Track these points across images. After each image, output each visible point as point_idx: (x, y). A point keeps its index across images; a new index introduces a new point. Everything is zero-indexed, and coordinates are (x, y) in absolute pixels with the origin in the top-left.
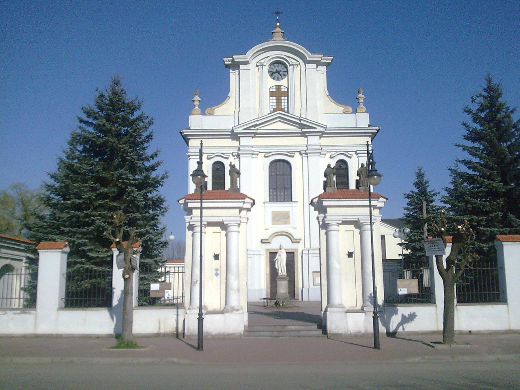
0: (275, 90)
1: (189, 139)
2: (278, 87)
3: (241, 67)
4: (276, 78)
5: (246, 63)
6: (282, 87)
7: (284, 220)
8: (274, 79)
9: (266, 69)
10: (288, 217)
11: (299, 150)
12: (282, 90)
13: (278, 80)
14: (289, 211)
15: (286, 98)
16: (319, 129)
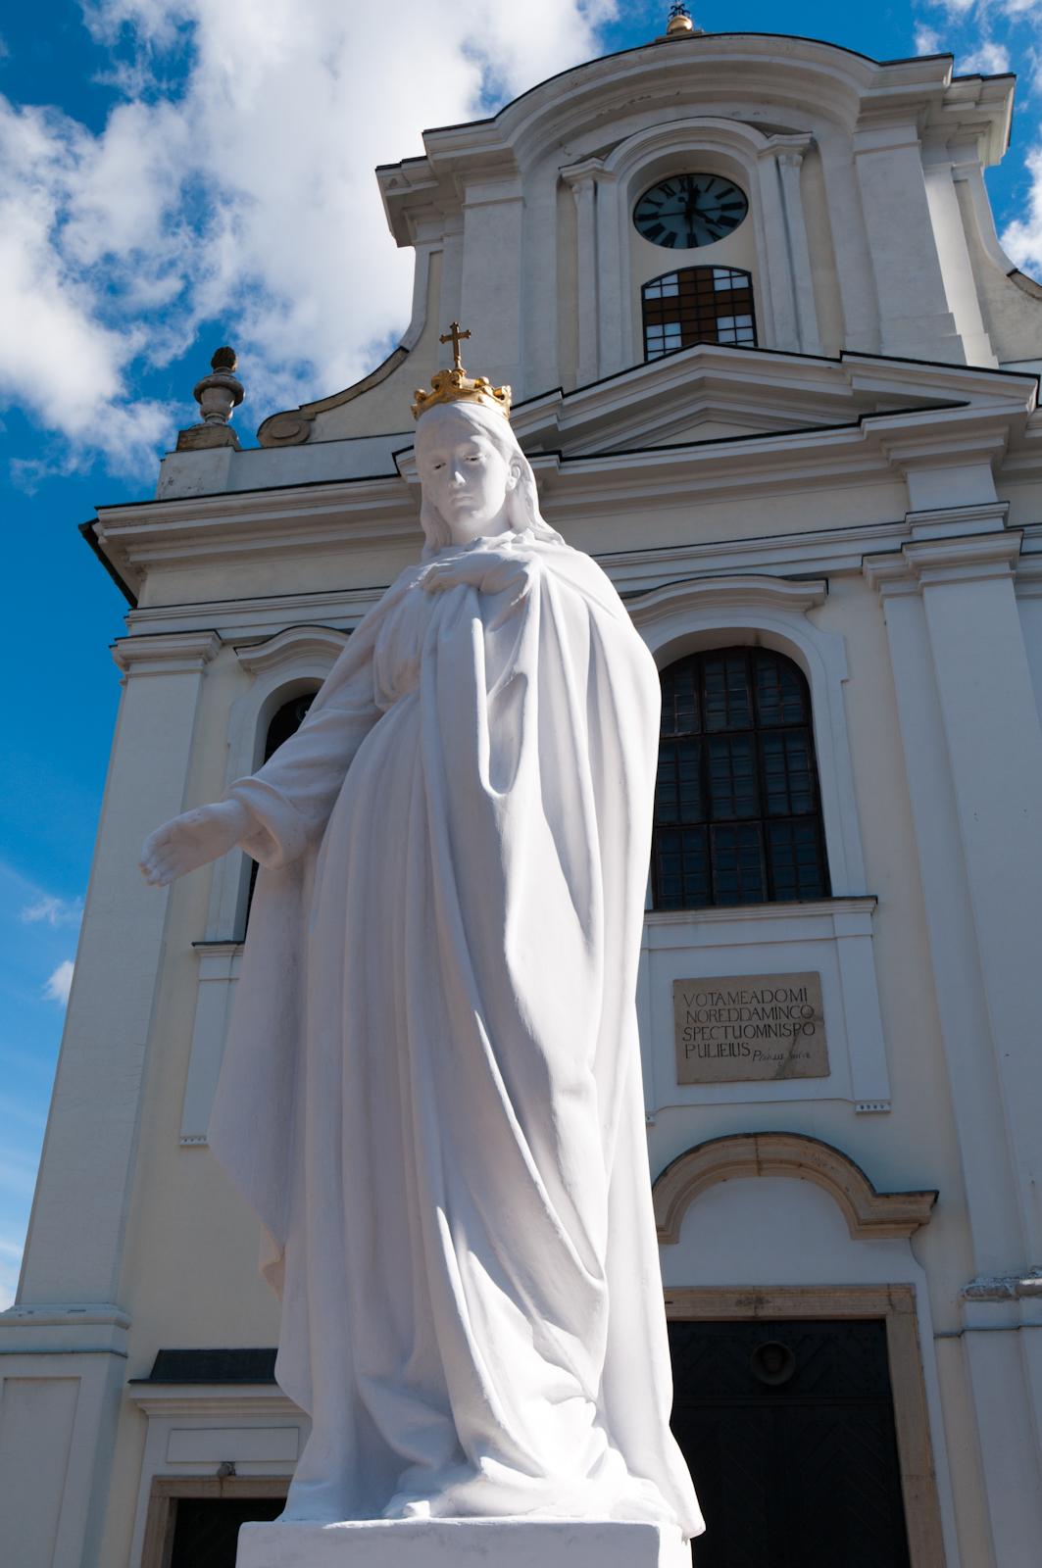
0: (672, 291)
1: (140, 570)
2: (695, 279)
3: (473, 194)
4: (681, 238)
5: (500, 166)
6: (717, 273)
7: (778, 1045)
8: (669, 242)
9: (617, 199)
10: (812, 1021)
11: (855, 563)
12: (721, 285)
13: (692, 243)
14: (814, 977)
15: (744, 320)
16: (982, 408)
